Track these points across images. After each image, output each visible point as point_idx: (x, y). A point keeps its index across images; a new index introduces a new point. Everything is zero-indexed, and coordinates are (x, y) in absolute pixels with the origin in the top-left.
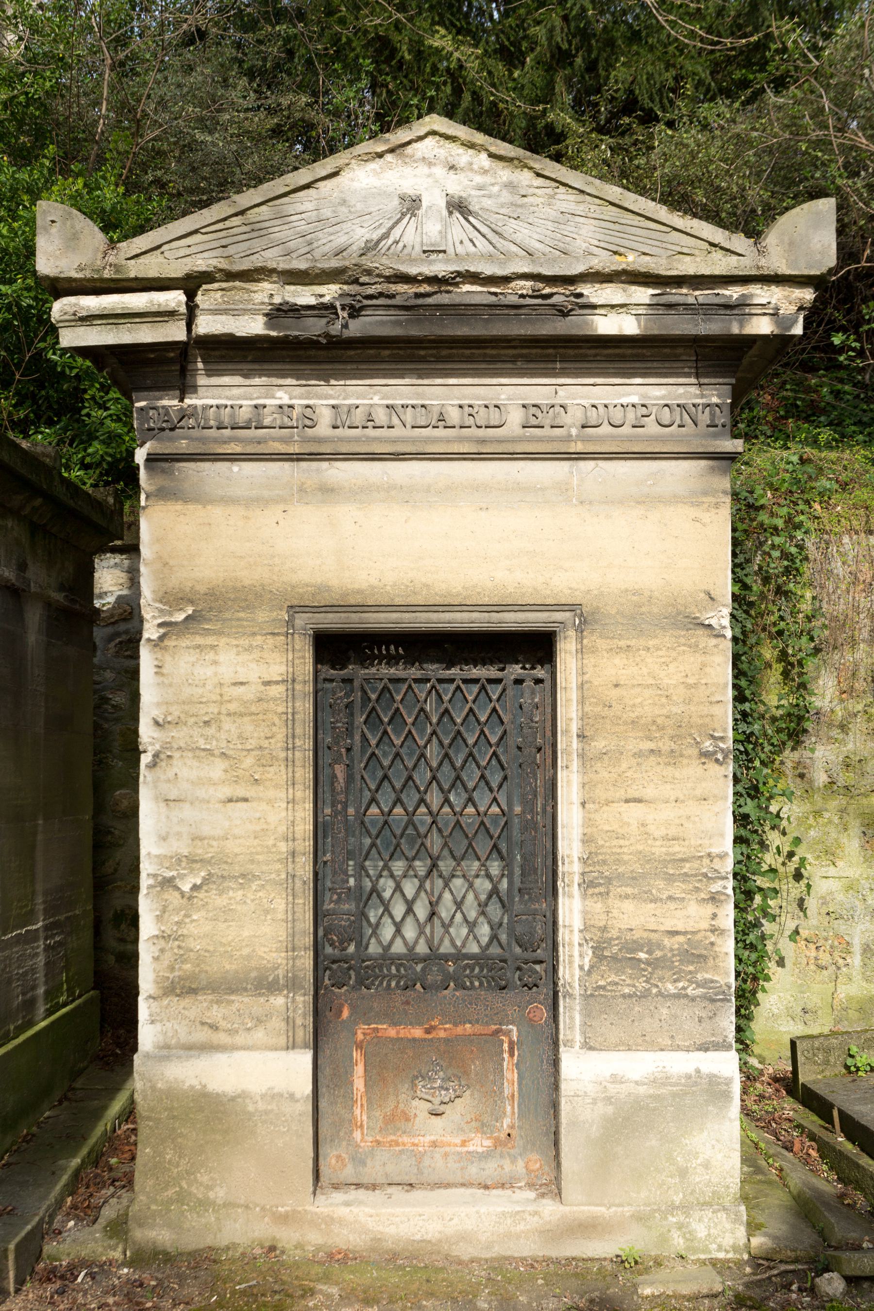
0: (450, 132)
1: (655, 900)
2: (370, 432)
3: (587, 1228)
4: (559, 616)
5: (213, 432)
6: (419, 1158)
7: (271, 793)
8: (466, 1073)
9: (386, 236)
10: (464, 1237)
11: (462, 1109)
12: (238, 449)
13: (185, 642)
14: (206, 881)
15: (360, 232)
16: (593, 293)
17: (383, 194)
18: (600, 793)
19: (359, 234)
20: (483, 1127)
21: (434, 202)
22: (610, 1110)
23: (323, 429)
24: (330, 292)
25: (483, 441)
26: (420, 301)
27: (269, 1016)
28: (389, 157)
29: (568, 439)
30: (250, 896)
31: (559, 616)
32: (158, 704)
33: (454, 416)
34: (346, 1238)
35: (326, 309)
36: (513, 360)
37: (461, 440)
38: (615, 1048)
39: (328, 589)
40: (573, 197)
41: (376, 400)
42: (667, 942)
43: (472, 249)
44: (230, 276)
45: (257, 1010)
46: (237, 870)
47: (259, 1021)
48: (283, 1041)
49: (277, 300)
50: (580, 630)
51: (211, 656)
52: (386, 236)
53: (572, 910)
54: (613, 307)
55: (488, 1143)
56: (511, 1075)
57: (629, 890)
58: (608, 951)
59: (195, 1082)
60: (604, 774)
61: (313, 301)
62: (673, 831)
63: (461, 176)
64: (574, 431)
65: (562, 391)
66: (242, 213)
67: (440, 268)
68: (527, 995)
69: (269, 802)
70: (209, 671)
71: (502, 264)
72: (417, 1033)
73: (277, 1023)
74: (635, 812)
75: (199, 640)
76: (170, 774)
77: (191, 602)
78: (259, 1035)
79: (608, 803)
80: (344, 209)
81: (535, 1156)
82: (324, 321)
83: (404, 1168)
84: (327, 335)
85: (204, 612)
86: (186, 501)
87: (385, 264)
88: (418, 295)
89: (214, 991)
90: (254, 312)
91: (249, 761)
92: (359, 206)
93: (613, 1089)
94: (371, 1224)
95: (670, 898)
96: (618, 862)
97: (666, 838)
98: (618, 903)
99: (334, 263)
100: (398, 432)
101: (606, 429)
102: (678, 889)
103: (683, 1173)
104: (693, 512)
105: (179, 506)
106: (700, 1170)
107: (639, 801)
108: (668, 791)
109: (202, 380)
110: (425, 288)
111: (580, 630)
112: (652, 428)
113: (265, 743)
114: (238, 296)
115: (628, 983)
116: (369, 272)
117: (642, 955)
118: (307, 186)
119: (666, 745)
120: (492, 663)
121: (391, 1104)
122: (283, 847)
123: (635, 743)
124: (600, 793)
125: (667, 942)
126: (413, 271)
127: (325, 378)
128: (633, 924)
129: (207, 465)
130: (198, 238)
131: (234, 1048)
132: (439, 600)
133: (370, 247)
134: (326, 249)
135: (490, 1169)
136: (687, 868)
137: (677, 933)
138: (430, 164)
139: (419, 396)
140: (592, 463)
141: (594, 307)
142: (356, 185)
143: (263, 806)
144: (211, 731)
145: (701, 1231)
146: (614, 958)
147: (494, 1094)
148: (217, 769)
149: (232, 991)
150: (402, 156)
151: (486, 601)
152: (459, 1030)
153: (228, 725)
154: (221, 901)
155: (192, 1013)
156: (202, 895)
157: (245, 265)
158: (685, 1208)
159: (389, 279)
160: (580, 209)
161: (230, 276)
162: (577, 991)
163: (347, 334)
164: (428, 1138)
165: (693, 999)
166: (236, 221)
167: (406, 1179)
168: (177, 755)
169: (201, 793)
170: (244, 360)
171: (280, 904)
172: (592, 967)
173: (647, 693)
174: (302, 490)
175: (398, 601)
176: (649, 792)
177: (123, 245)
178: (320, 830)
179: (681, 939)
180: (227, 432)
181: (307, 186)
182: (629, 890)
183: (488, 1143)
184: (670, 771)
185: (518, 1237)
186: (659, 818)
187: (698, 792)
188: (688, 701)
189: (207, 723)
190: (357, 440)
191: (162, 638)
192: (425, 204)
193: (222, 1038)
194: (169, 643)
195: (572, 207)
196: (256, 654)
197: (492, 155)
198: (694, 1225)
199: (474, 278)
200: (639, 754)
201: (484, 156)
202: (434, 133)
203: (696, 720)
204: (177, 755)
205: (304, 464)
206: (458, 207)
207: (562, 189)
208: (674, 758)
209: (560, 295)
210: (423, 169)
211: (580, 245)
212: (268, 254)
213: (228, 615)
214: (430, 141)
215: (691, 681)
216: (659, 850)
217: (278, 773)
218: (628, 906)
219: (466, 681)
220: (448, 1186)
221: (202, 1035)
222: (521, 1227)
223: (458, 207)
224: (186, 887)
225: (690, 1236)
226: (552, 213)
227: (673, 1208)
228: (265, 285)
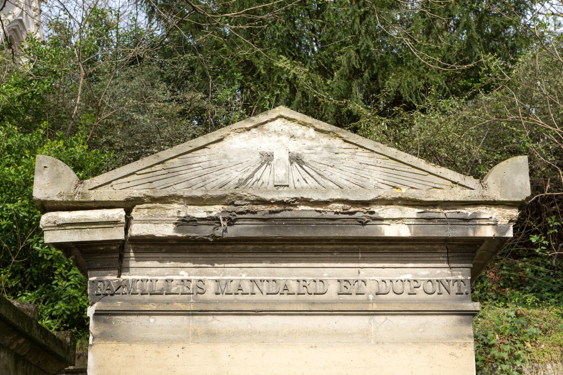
0: (291, 116)
2: (240, 297)
5: (138, 297)
9: (251, 176)
12: (154, 308)
19: (235, 175)
23: (210, 295)
24: (216, 210)
25: (313, 303)
26: (272, 216)
28: (254, 130)
29: (368, 301)
33: (294, 287)
36: (331, 252)
37: (298, 302)
40: (367, 154)
41: (244, 276)
43: (305, 184)
44: (154, 200)
49: (183, 214)
52: (251, 176)
54: (393, 219)
61: (205, 215)
63: (298, 142)
64: (371, 297)
65: (363, 272)
66: (163, 162)
67: (285, 196)
71: (324, 193)
80: (226, 161)
82: (212, 227)
84: (213, 236)
86: (119, 341)
87: (251, 193)
88: (271, 212)
90: (167, 222)
92: (235, 159)
99: (219, 193)
100: (258, 297)
101: (391, 295)
104: (450, 349)
105: (114, 345)
109: (133, 264)
110: (276, 208)
116: (240, 198)
118: (203, 147)
126: (268, 197)
127: (212, 262)
129: (133, 318)
130: (134, 177)
133: (242, 183)
134: (214, 184)
138: (279, 135)
139: (271, 274)
140: (383, 318)
141: (382, 219)
142: (233, 147)
150: (262, 129)
157: (163, 193)
159: (253, 202)
160: (371, 161)
161: (154, 200)
163: (226, 235)
170: (160, 251)
174: (195, 334)
180: (147, 297)
181: (203, 147)
190: (231, 302)
192: (275, 158)
195: (367, 160)
197: (316, 130)
199: (306, 202)
201: (312, 130)
202: (281, 117)
205: (196, 318)
206: (296, 159)
207: (360, 150)
210: (275, 138)
211: (372, 182)
212: (178, 187)
214: (279, 121)
223: (296, 159)
226: (355, 164)
228: (175, 205)
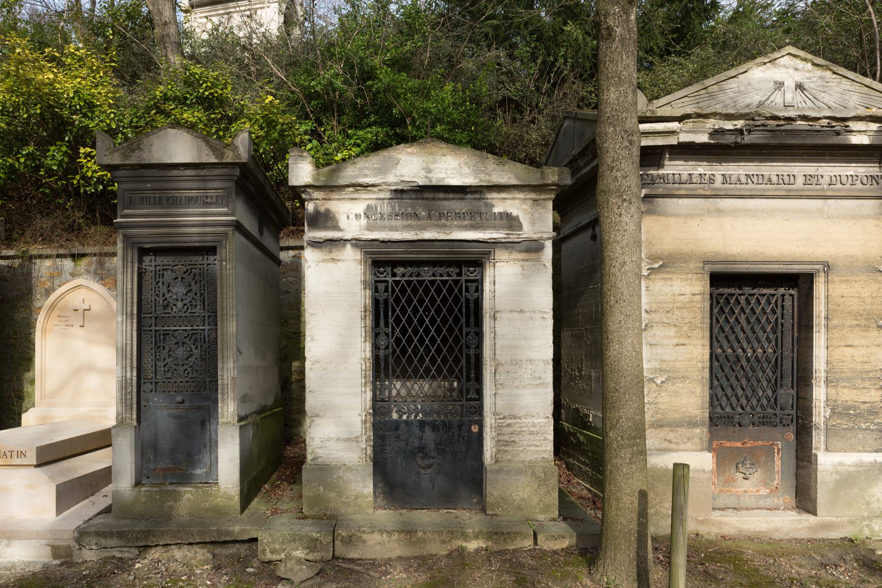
0: (797, 53)
1: (857, 389)
2: (738, 186)
3: (828, 526)
4: (817, 267)
5: (670, 185)
6: (739, 497)
7: (695, 342)
8: (759, 462)
9: (768, 99)
10: (776, 530)
11: (757, 476)
12: (684, 193)
13: (658, 277)
14: (667, 379)
15: (757, 97)
16: (854, 126)
17: (766, 81)
18: (835, 343)
19: (755, 98)
20: (765, 484)
21: (790, 84)
22: (838, 477)
23: (718, 184)
24: (740, 124)
25: (790, 190)
26: (778, 128)
27: (693, 437)
28: (768, 65)
29: (823, 190)
30: (686, 386)
31: (817, 267)
32: (647, 303)
33: (774, 179)
34: (728, 531)
35: (740, 132)
36: (802, 155)
37: (775, 190)
38: (839, 451)
39: (720, 254)
40: (849, 83)
41: (741, 172)
42: (862, 406)
43: (804, 105)
44: (699, 116)
45: (688, 435)
46: (680, 375)
47: (689, 439)
48: (699, 447)
49: (716, 127)
50: (827, 273)
51: (669, 282)
52: (768, 99)
53: (819, 393)
54: (860, 131)
55: (768, 491)
56: (778, 463)
57: (846, 384)
58: (837, 410)
59: (663, 465)
60: (836, 334)
61: (732, 128)
62: (865, 359)
63: (800, 73)
64: (825, 187)
65: (820, 169)
66: (705, 88)
67: (792, 113)
68: (785, 429)
69: (694, 345)
70: (669, 289)
71: (819, 112)
72: (739, 445)
73: (696, 440)
74: (849, 351)
75: (664, 276)
76: (652, 333)
77: (661, 259)
78: (689, 445)
79: (838, 347)
80: (750, 87)
81: (787, 497)
82: (734, 136)
83: (732, 502)
84: (736, 143)
85: (666, 264)
86: (659, 215)
87: (767, 112)
88: (778, 126)
89: (670, 426)
90: (704, 132)
91: (686, 328)
92: (756, 86)
93: (839, 468)
94: (737, 524)
95: (864, 388)
96: (842, 372)
97: (862, 362)
98: (841, 390)
99: (747, 111)
100: (751, 186)
101: (839, 186)
102: (867, 384)
103: (868, 503)
104: (875, 222)
105: (656, 218)
106: (875, 502)
107: (851, 346)
108: (864, 342)
109: (667, 163)
110: (782, 122)
111: (827, 273)
112: (859, 185)
113: (693, 321)
114: (699, 125)
115: (845, 423)
116: (760, 115)
117: (852, 412)
118: (734, 77)
119: (863, 323)
120: (771, 287)
121: (727, 474)
122: (700, 365)
123: (850, 322)
124: (835, 343)
125: (862, 406)
126: (781, 114)
127: (720, 162)
128: (848, 399)
129: (668, 200)
130: (686, 99)
131: (679, 450)
132: (767, 259)
133: (761, 104)
134: (742, 104)
135: (769, 502)
136: (871, 375)
137: (866, 402)
138: (787, 68)
139: (759, 171)
140: (833, 201)
141: (852, 131)
142: (755, 77)
143: (692, 347)
144: (670, 315)
145: (877, 528)
146: (840, 413)
147: (770, 471)
148: (672, 331)
149: (678, 426)
150: (774, 64)
151: (787, 260)
152: (756, 444)
153: (676, 312)
154: (673, 388)
155: (660, 436)
156: (665, 385)
157: (708, 111)
158: (869, 518)
159: (767, 118)
160: (852, 88)
161: (699, 116)
162: (822, 426)
163: (744, 142)
164: (743, 489)
165: (872, 431)
166: (703, 92)
167: (733, 506)
168: (655, 325)
169: (665, 342)
170: (687, 154)
171: (698, 390)
172: (830, 417)
173: (855, 300)
174: (709, 211)
175: (750, 259)
176: (856, 343)
177: (655, 101)
178: (713, 357)
179: (868, 405)
180: (676, 185)
181: (734, 77)
182: (846, 384)
183: (768, 491)
184: (864, 334)
185: (800, 530)
186: (859, 354)
187: (876, 343)
188: (872, 304)
189: (668, 312)
190: (732, 189)
191: (649, 275)
192: (786, 85)
193: (673, 446)
194: (652, 277)
195: (848, 87)
196: (689, 282)
197: (814, 64)
198: (874, 525)
199: (805, 118)
200: (851, 326)
201: (810, 64)
202: (789, 54)
203: (876, 312)
204: (655, 325)
205: (710, 200)
206: (800, 87)
207: (844, 79)
208: (866, 328)
209: (838, 126)
210: (784, 70)
211: (851, 104)
212: (717, 106)
213: (677, 265)
214: (786, 58)
215: (874, 295)
216: (859, 367)
217: (698, 333)
218: (846, 391)
219: (760, 295)
220: (753, 509)
221: (665, 445)
222: (800, 526)
223: (800, 87)
224: (659, 382)
225: (872, 530)
226: (840, 91)
227: (864, 518)
228: (711, 120)
